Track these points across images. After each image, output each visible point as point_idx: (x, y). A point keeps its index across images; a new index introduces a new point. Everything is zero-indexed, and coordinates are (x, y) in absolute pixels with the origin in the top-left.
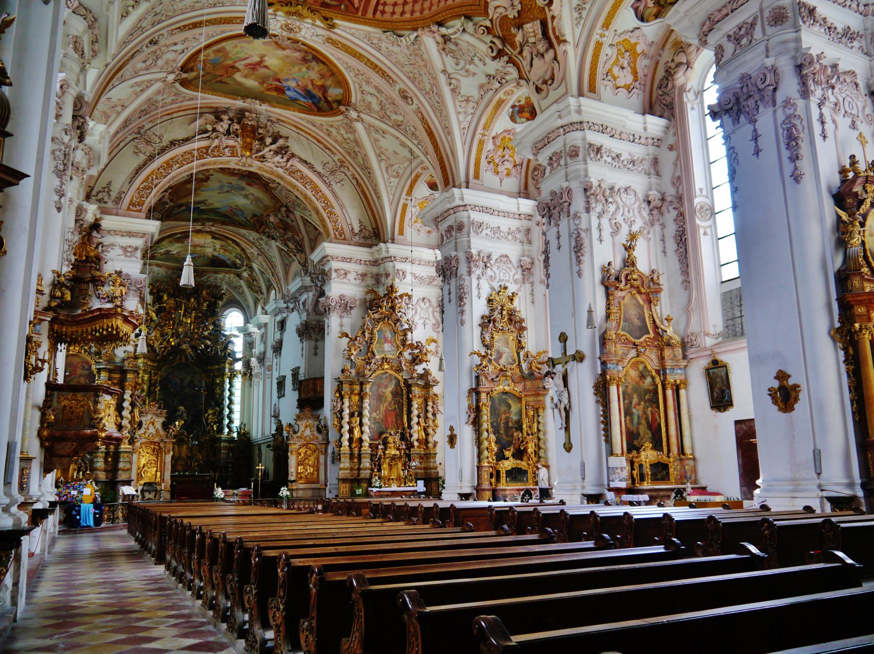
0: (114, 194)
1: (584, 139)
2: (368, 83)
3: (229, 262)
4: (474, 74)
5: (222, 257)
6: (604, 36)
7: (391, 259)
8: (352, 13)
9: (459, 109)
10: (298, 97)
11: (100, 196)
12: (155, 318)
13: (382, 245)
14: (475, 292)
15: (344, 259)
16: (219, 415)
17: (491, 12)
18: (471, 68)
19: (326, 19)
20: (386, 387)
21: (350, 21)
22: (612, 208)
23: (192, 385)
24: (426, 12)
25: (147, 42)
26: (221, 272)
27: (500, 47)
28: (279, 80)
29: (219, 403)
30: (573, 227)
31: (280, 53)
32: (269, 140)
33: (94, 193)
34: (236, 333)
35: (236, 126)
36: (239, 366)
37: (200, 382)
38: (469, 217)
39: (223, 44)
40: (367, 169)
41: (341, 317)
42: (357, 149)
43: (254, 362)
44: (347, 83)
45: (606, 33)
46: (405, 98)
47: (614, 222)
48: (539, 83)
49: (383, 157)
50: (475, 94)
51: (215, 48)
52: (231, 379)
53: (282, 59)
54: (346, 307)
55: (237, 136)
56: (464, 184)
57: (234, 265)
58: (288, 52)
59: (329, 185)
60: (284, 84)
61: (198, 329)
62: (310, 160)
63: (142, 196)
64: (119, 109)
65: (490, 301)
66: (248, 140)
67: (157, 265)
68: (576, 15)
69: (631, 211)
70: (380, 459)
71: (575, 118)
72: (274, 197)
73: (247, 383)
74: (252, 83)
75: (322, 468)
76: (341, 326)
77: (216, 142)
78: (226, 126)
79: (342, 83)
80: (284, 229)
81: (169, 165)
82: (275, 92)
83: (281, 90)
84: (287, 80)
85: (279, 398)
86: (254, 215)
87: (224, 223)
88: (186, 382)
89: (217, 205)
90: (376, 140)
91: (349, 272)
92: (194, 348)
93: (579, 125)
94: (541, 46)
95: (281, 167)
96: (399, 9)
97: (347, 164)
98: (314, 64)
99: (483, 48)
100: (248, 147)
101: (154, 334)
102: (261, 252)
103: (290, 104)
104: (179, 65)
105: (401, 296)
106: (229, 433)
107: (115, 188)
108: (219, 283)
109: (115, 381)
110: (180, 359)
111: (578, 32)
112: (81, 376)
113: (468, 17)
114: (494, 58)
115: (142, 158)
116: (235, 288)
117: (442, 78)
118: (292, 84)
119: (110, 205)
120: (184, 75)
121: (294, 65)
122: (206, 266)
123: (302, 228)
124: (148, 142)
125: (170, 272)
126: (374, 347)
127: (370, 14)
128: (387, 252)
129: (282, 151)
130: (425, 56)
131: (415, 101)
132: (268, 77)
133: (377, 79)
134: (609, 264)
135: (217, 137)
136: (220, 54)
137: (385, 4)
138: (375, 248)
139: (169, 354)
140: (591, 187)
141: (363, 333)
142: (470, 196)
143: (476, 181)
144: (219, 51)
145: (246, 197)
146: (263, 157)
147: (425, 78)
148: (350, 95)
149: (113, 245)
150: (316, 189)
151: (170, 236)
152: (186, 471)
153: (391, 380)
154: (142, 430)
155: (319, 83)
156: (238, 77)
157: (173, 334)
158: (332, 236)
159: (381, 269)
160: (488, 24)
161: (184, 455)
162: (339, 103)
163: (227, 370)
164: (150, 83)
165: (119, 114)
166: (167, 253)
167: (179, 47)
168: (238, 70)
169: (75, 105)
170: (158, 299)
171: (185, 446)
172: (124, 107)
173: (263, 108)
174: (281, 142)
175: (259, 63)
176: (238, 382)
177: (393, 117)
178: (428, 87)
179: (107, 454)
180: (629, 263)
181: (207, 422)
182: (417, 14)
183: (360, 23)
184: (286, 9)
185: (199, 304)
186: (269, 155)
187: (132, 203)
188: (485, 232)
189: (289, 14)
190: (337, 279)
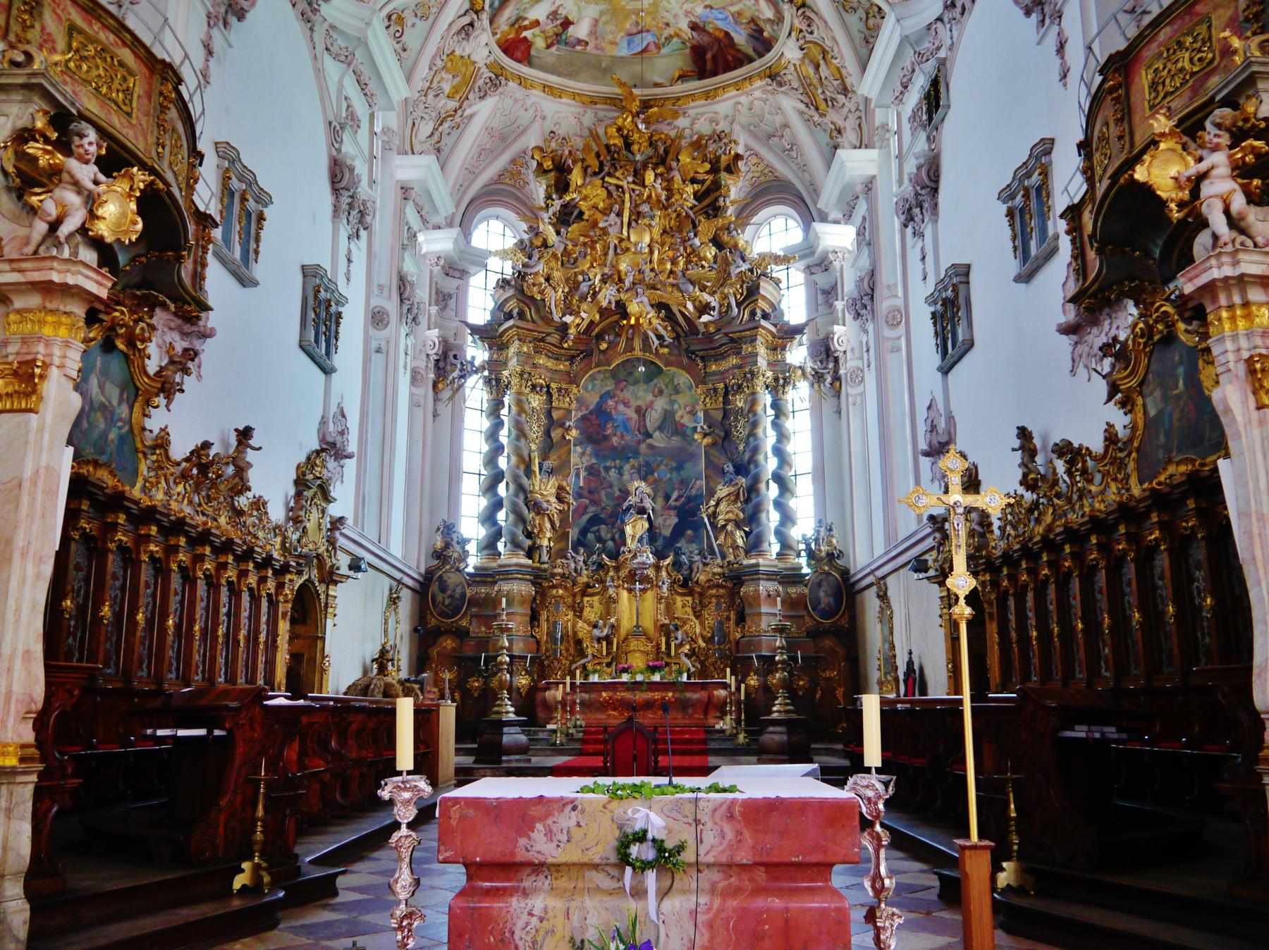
3: (741, 38)
16: (747, 501)
23: (669, 423)
29: (746, 467)
36: (798, 354)
37: (693, 413)
43: (844, 334)
52: (779, 385)
61: (674, 262)
67: (547, 89)
73: (829, 405)
85: (945, 370)
88: (653, 419)
92: (660, 306)
101: (540, 268)
106: (780, 555)
108: (723, 126)
116: (770, 136)
122: (683, 77)
125: (588, 119)
152: (653, 669)
157: (604, 281)
161: (648, 623)
163: (762, 363)
170: (562, 186)
171: (650, 595)
176: (799, 395)
181: (713, 525)
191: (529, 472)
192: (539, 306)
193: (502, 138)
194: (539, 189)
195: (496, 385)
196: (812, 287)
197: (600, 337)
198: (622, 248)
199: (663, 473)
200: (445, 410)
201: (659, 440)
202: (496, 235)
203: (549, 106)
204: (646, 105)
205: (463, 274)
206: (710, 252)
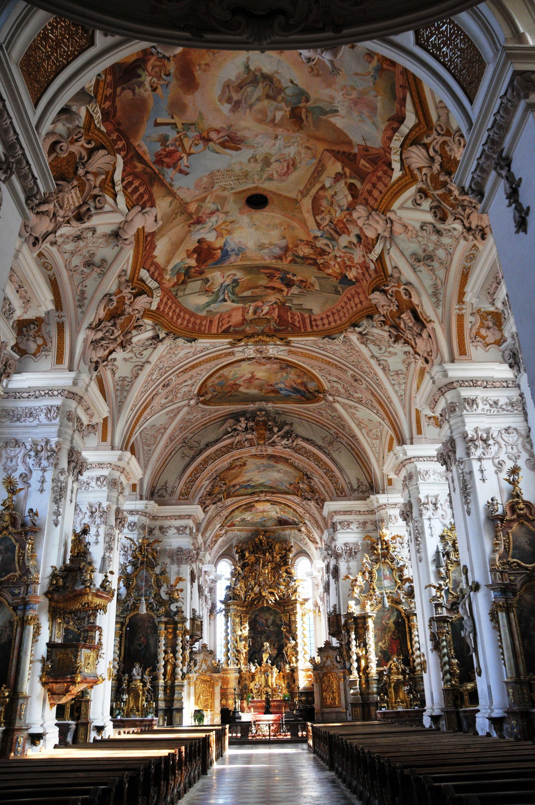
0: (169, 490)
1: (459, 396)
2: (330, 374)
4: (395, 354)
5: (284, 517)
6: (462, 309)
7: (381, 507)
8: (298, 332)
9: (393, 382)
10: (289, 393)
11: (160, 492)
12: (241, 572)
13: (372, 497)
14: (427, 531)
15: (345, 513)
17: (380, 310)
18: (391, 349)
19: (282, 339)
20: (389, 619)
21: (298, 336)
22: (494, 449)
24: (343, 319)
25: (160, 386)
26: (287, 528)
27: (395, 333)
28: (271, 385)
30: (460, 471)
31: (263, 368)
32: (276, 429)
33: (156, 491)
34: (305, 577)
35: (252, 424)
38: (416, 467)
39: (221, 372)
40: (354, 436)
41: (348, 562)
42: (343, 423)
44: (317, 378)
45: (464, 306)
46: (356, 380)
47: (496, 461)
48: (425, 355)
49: (362, 425)
50: (403, 367)
51: (217, 375)
53: (266, 371)
54: (351, 553)
55: (253, 431)
56: (408, 441)
57: (295, 523)
58: (268, 366)
59: (328, 455)
60: (276, 387)
62: (312, 437)
63: (188, 488)
64: (162, 431)
65: (442, 537)
66: (262, 432)
68: (434, 300)
69: (515, 447)
70: (385, 684)
71: (446, 381)
72: (296, 468)
74: (253, 391)
75: (342, 693)
76: (349, 568)
77: (238, 438)
78: (244, 425)
79: (313, 378)
80: (313, 492)
81: (205, 462)
82: (273, 393)
83: (276, 391)
84: (277, 384)
86: (291, 484)
87: (273, 493)
89: (262, 481)
90: (353, 414)
91: (352, 523)
93: (450, 386)
94: (416, 329)
95: (289, 448)
96: (326, 321)
97: (341, 435)
98: (289, 369)
99: (386, 334)
100: (261, 437)
102: (307, 511)
103: (286, 399)
104: (196, 392)
105: (393, 538)
107: (170, 484)
109: (170, 630)
110: (263, 603)
111: (440, 311)
112: (148, 627)
113: (370, 317)
114: (395, 342)
115: (187, 459)
117: (373, 362)
118: (282, 386)
119: (167, 497)
120: (202, 399)
121: (276, 373)
123: (322, 489)
124: (191, 448)
126: (374, 584)
127: (309, 329)
128: (378, 502)
129: (287, 435)
130: (357, 349)
131: (364, 382)
132: (263, 385)
133: (334, 371)
134: (492, 499)
135: (238, 435)
136: (222, 379)
137: (315, 320)
138: (368, 500)
139: (253, 600)
140: (467, 436)
141: (364, 573)
142: (411, 450)
143: (419, 436)
144: (220, 377)
145: (278, 471)
146: (274, 442)
147: (363, 363)
148: (322, 385)
149: (170, 527)
150: (318, 460)
151: (237, 508)
153: (393, 612)
154: (197, 667)
155: (299, 381)
156: (242, 389)
157: (255, 584)
158: (335, 495)
159: (377, 517)
160: (382, 319)
162: (318, 392)
164: (179, 410)
165: (163, 434)
166: (243, 520)
167: (189, 382)
168: (240, 386)
169: (69, 455)
170: (242, 557)
172: (166, 429)
173: (270, 406)
174: (286, 428)
175: (253, 377)
177: (356, 395)
178: (367, 370)
179: (165, 687)
180: (515, 495)
182: (339, 322)
183: (305, 336)
184: (252, 340)
185: (273, 557)
186: (278, 440)
187: (182, 494)
188: (432, 477)
189: (256, 343)
190: (341, 531)
191: (237, 642)
192: (239, 596)
193: (225, 543)
194: (237, 556)
195: (226, 616)
196: (313, 582)
197: (254, 601)
198: (261, 574)
199: (273, 638)
200: (212, 623)
201: (271, 629)
202: (225, 568)
203: (238, 533)
204: (266, 532)
205: (216, 581)
206: (285, 575)
